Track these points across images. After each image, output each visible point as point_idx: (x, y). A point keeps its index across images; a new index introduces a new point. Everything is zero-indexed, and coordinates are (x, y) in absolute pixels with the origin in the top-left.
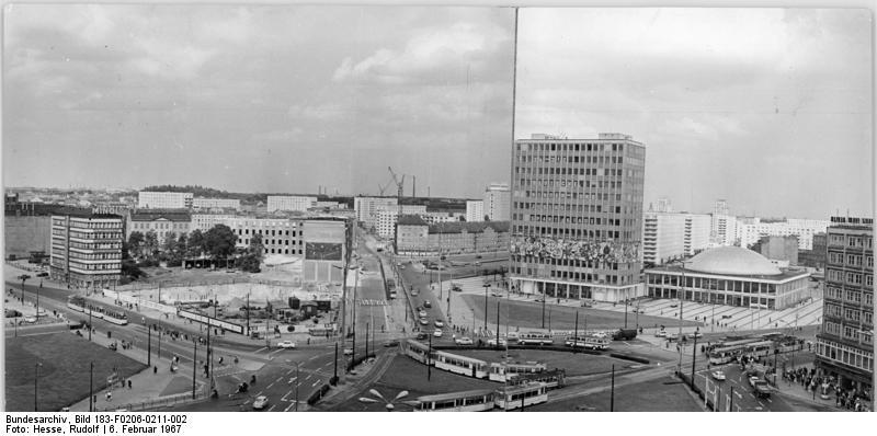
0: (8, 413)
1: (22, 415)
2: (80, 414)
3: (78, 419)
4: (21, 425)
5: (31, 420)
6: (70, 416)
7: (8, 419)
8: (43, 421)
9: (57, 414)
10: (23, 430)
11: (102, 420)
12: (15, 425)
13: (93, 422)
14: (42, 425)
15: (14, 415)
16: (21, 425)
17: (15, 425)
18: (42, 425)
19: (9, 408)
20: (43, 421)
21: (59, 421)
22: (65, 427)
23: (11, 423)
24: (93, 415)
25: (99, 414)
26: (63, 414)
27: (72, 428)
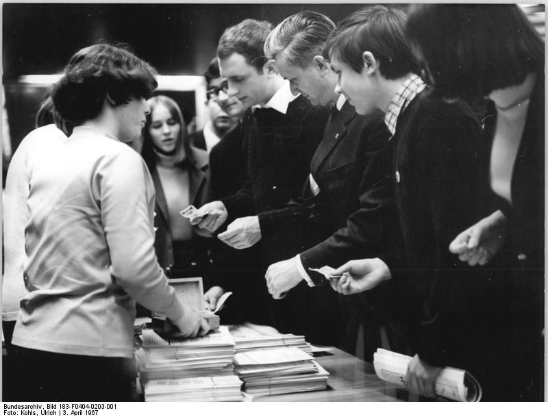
0: (5, 403)
1: (14, 404)
2: (48, 403)
3: (48, 407)
4: (13, 410)
5: (19, 407)
6: (44, 405)
7: (5, 406)
8: (27, 407)
9: (36, 403)
10: (14, 414)
11: (64, 406)
12: (10, 410)
13: (57, 410)
14: (27, 410)
15: (9, 404)
16: (13, 410)
17: (10, 410)
18: (27, 410)
19: (4, 400)
20: (27, 407)
21: (37, 408)
22: (38, 411)
23: (7, 409)
24: (58, 404)
25: (62, 403)
26: (40, 404)
27: (46, 413)
